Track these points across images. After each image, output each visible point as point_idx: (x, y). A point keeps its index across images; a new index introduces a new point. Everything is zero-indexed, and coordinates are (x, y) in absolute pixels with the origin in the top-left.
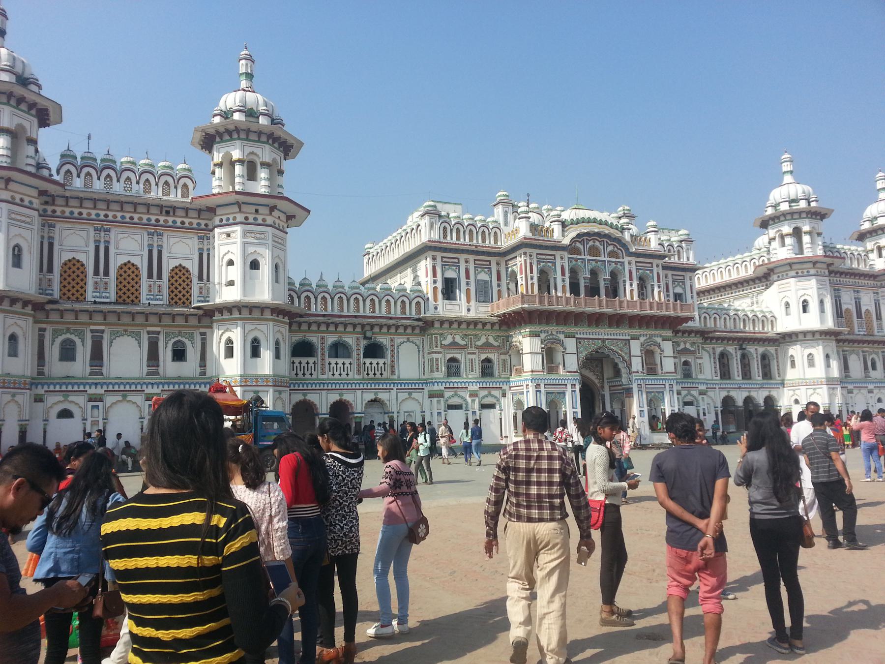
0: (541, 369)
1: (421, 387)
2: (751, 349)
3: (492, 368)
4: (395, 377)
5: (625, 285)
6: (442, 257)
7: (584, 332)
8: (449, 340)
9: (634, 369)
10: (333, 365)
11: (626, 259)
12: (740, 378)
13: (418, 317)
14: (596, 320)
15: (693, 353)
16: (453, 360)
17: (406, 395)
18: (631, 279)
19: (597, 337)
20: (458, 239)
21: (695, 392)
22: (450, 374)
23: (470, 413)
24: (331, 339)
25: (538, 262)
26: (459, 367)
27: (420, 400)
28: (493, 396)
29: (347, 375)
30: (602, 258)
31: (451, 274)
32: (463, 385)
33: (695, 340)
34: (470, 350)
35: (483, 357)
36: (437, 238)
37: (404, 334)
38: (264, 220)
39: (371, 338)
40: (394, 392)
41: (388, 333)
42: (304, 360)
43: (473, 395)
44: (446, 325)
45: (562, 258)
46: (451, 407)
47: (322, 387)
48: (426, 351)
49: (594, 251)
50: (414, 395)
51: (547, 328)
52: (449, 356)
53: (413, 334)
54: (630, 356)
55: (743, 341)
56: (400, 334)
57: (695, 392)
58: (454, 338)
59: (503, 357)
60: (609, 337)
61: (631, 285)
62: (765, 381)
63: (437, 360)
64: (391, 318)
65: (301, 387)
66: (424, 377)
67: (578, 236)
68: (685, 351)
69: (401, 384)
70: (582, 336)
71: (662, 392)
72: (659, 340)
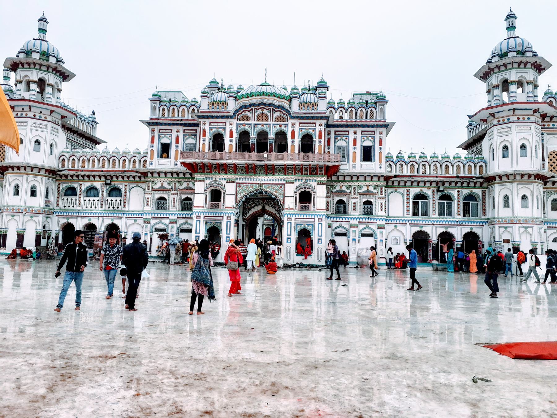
2: (453, 192)
4: (126, 209)
6: (160, 129)
7: (241, 178)
8: (158, 185)
9: (286, 206)
10: (87, 201)
11: (290, 122)
12: (437, 215)
14: (250, 169)
15: (375, 194)
16: (162, 199)
17: (133, 221)
18: (293, 135)
19: (255, 182)
21: (374, 227)
24: (86, 185)
25: (211, 128)
26: (165, 204)
28: (188, 224)
30: (269, 123)
31: (165, 141)
32: (165, 216)
33: (378, 184)
35: (184, 196)
37: (134, 181)
38: (27, 115)
41: (123, 181)
42: (70, 198)
43: (173, 222)
44: (156, 175)
45: (231, 124)
47: (77, 215)
49: (263, 117)
50: (138, 221)
51: (210, 176)
52: (158, 196)
53: (140, 181)
55: (439, 184)
56: (132, 182)
57: (374, 227)
58: (162, 184)
60: (266, 182)
62: (466, 219)
63: (148, 198)
64: (125, 171)
65: (65, 214)
67: (245, 106)
68: (368, 193)
71: (312, 225)
72: (314, 184)
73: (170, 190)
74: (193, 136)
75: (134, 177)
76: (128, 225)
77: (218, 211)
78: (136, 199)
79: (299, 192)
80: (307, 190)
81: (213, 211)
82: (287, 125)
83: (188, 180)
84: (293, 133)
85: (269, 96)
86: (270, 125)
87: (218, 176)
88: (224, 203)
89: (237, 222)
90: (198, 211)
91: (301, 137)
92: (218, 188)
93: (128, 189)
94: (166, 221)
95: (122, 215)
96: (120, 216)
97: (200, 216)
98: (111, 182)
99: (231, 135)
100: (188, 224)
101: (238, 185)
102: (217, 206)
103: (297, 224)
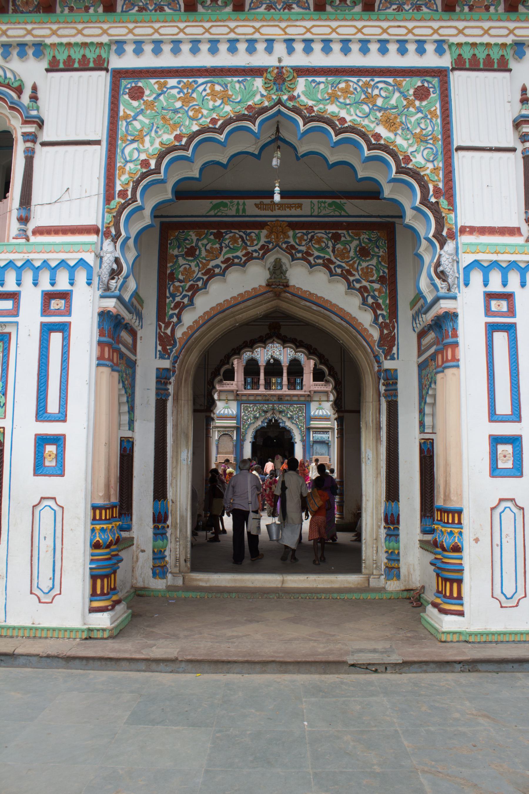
19: (241, 59)
60: (318, 59)
70: (147, 61)
88: (26, 199)
89: (115, 331)
101: (126, 84)
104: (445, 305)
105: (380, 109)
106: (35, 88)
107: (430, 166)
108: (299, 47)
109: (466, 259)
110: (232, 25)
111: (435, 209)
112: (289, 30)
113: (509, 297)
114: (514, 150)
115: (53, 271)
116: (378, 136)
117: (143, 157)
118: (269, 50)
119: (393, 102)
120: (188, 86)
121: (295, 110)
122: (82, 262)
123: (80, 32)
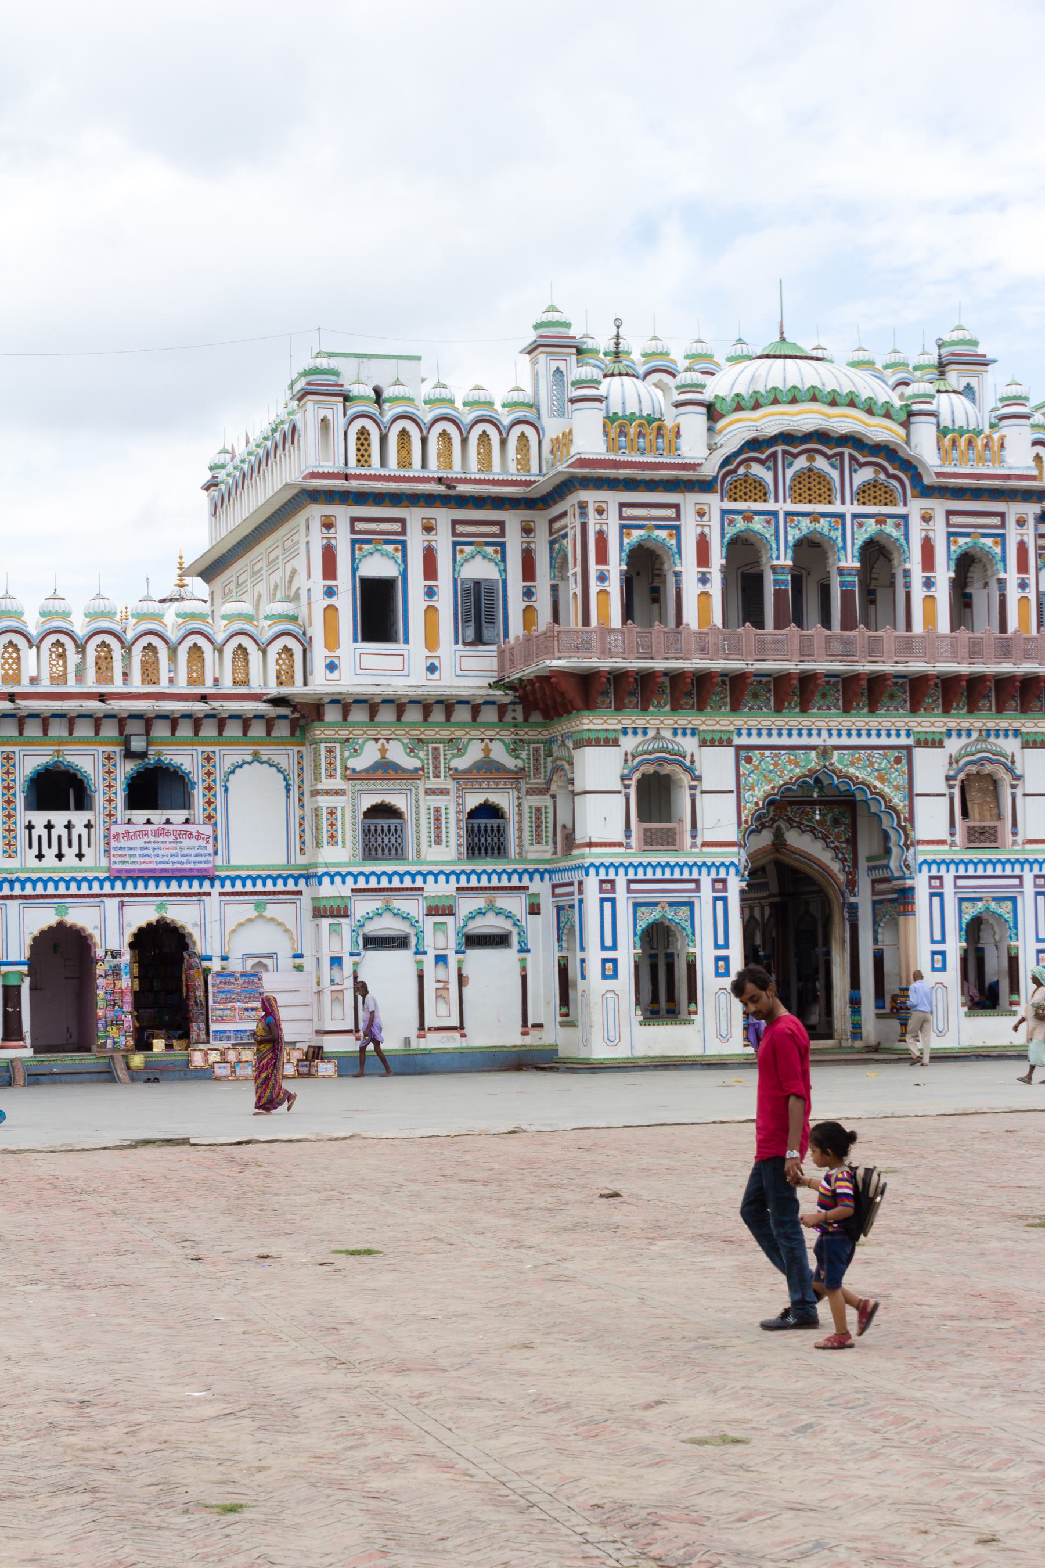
0: (620, 837)
1: (291, 886)
3: (500, 832)
5: (908, 585)
6: (353, 520)
8: (368, 757)
10: (39, 830)
11: (915, 507)
13: (285, 691)
16: (383, 811)
18: (928, 563)
19: (805, 741)
20: (405, 462)
22: (370, 852)
23: (429, 961)
24: (32, 761)
25: (624, 529)
26: (399, 832)
27: (291, 925)
28: (499, 912)
29: (80, 856)
30: (836, 508)
32: (408, 883)
34: (433, 783)
35: (473, 801)
36: (335, 465)
39: (143, 755)
40: (213, 902)
43: (439, 910)
44: (359, 715)
45: (701, 514)
46: (374, 943)
48: (307, 789)
49: (811, 486)
51: (641, 721)
52: (368, 802)
54: (911, 795)
56: (232, 742)
58: (383, 751)
59: (535, 801)
60: (844, 741)
61: (928, 583)
63: (332, 813)
64: (204, 698)
66: (302, 860)
67: (754, 444)
69: (233, 880)
70: (754, 740)
71: (1013, 900)
72: (1010, 746)
73: (415, 775)
74: (490, 550)
75: (246, 722)
76: (230, 926)
77: (681, 861)
78: (251, 812)
79: (962, 776)
80: (988, 768)
81: (663, 860)
82: (905, 517)
83: (491, 733)
84: (928, 548)
85: (833, 403)
86: (842, 516)
87: (669, 721)
90: (607, 861)
91: (953, 567)
92: (667, 769)
93: (218, 775)
94: (413, 907)
95: (206, 886)
96: (196, 888)
97: (612, 882)
98: (149, 743)
99: (703, 559)
100: (499, 912)
102: (667, 840)
103: (961, 900)
104: (909, 882)
105: (877, 770)
106: (692, 756)
107: (902, 804)
108: (834, 732)
109: (921, 859)
110: (800, 720)
111: (904, 829)
112: (831, 724)
113: (940, 878)
114: (944, 795)
115: (718, 868)
116: (875, 787)
117: (755, 800)
118: (819, 735)
119: (883, 766)
120: (776, 755)
121: (833, 772)
122: (732, 864)
123: (718, 723)
